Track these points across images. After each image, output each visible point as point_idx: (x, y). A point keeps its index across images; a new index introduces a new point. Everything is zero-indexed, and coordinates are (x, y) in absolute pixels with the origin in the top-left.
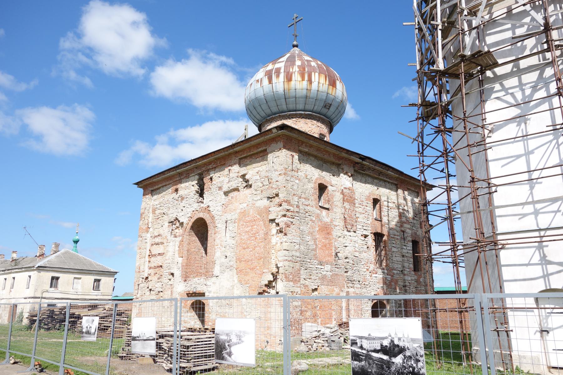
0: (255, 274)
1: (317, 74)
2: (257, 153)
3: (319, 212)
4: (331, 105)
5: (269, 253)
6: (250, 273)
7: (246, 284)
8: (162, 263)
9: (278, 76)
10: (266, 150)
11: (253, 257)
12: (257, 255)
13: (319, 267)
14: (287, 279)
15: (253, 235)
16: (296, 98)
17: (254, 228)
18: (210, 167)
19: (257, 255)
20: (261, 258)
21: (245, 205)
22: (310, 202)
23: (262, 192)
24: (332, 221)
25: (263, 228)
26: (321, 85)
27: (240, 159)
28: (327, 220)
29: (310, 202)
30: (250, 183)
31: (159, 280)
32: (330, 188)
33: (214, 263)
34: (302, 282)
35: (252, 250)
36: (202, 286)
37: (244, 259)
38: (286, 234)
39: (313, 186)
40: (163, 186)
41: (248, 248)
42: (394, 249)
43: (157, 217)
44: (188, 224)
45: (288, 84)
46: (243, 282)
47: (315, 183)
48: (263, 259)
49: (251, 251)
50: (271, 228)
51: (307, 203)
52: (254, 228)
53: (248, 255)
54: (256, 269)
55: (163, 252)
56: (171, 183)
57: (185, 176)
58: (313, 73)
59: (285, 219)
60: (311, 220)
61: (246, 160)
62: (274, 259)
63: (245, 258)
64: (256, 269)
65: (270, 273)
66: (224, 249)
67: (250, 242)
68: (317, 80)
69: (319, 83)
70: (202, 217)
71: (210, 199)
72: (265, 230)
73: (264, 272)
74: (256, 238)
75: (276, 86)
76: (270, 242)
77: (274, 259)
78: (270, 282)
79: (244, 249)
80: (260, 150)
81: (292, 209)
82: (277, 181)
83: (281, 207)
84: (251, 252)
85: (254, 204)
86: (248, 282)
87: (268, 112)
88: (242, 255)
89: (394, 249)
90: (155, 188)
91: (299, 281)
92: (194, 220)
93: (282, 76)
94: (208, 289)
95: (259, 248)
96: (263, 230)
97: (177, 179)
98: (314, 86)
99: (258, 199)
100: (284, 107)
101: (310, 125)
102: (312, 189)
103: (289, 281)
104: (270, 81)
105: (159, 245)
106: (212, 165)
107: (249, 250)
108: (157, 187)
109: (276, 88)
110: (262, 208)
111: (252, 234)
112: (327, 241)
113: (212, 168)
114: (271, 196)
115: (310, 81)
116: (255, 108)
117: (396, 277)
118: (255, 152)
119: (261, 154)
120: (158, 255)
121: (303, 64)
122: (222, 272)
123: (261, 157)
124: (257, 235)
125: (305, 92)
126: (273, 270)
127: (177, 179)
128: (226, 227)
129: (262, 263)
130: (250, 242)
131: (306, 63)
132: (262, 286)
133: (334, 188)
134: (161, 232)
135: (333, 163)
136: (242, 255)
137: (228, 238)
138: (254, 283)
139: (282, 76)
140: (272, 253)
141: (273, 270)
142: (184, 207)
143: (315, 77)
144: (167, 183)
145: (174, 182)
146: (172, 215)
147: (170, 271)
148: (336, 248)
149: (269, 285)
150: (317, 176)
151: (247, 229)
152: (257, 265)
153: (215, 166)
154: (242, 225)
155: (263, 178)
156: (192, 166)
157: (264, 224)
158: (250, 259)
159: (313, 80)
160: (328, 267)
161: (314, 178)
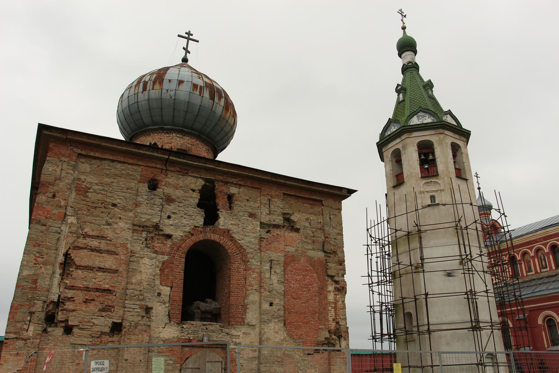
0: (309, 329)
2: (305, 198)
5: (325, 309)
6: (303, 327)
7: (299, 338)
8: (111, 286)
11: (306, 310)
12: (311, 309)
15: (305, 286)
16: (222, 129)
17: (307, 279)
18: (234, 180)
19: (311, 309)
20: (316, 313)
21: (293, 249)
23: (314, 242)
25: (317, 281)
30: (298, 226)
31: (104, 314)
35: (304, 301)
36: (220, 336)
37: (295, 311)
40: (113, 161)
41: (299, 298)
43: (94, 205)
44: (183, 240)
45: (225, 113)
46: (294, 337)
48: (318, 314)
49: (303, 303)
50: (327, 283)
52: (307, 279)
53: (300, 306)
54: (310, 324)
55: (114, 267)
56: (140, 165)
57: (178, 169)
61: (289, 198)
62: (331, 316)
63: (296, 309)
64: (310, 324)
65: (327, 330)
66: (268, 294)
67: (302, 293)
70: (218, 240)
71: (232, 222)
72: (319, 283)
73: (320, 328)
74: (309, 290)
75: (216, 106)
76: (326, 298)
77: (331, 316)
79: (294, 299)
80: (314, 197)
82: (336, 239)
83: (341, 267)
84: (304, 305)
85: (305, 252)
86: (302, 337)
88: (292, 305)
90: (92, 154)
92: (198, 240)
94: (234, 340)
95: (313, 302)
96: (318, 283)
97: (158, 166)
99: (309, 248)
105: (102, 253)
106: (237, 180)
107: (301, 301)
108: (97, 155)
109: (215, 109)
110: (316, 259)
111: (304, 285)
113: (235, 184)
114: (328, 252)
116: (174, 109)
118: (307, 196)
119: (311, 202)
120: (97, 270)
122: (262, 322)
123: (310, 204)
124: (311, 287)
126: (331, 327)
127: (158, 166)
128: (271, 268)
129: (317, 318)
130: (302, 293)
132: (320, 343)
134: (109, 234)
136: (292, 305)
137: (275, 281)
138: (309, 338)
140: (329, 310)
141: (331, 327)
142: (174, 213)
144: (130, 161)
145: (148, 166)
146: (150, 217)
147: (143, 303)
151: (298, 278)
152: (311, 319)
153: (242, 183)
154: (291, 271)
155: (314, 228)
156: (206, 165)
157: (319, 278)
158: (302, 311)
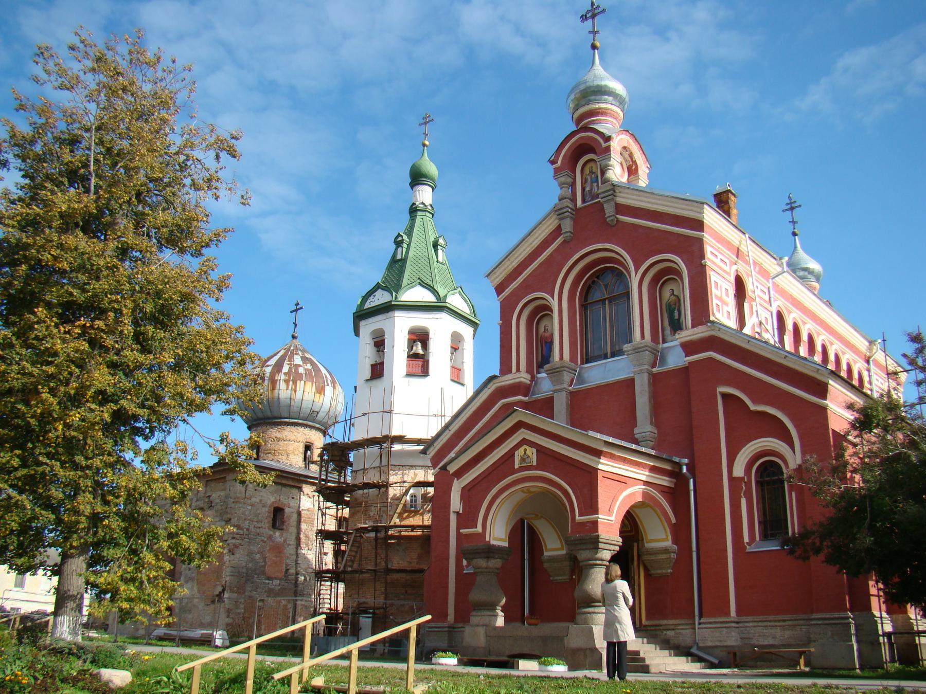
2: (220, 478)
3: (271, 533)
4: (318, 412)
10: (225, 477)
13: (267, 581)
14: (232, 591)
22: (262, 525)
24: (285, 541)
26: (306, 394)
27: (207, 481)
28: (281, 540)
29: (262, 525)
32: (287, 510)
33: (181, 573)
34: (246, 593)
38: (233, 554)
39: (267, 509)
47: (270, 507)
51: (259, 525)
58: (298, 382)
59: (234, 541)
60: (262, 541)
78: (220, 593)
81: (241, 532)
87: (255, 417)
91: (244, 593)
98: (299, 394)
100: (269, 414)
101: (295, 433)
102: (265, 513)
103: (233, 592)
112: (278, 559)
121: (290, 369)
133: (291, 510)
135: (294, 487)
148: (287, 565)
149: (220, 596)
150: (273, 499)
160: (277, 582)
161: (269, 502)
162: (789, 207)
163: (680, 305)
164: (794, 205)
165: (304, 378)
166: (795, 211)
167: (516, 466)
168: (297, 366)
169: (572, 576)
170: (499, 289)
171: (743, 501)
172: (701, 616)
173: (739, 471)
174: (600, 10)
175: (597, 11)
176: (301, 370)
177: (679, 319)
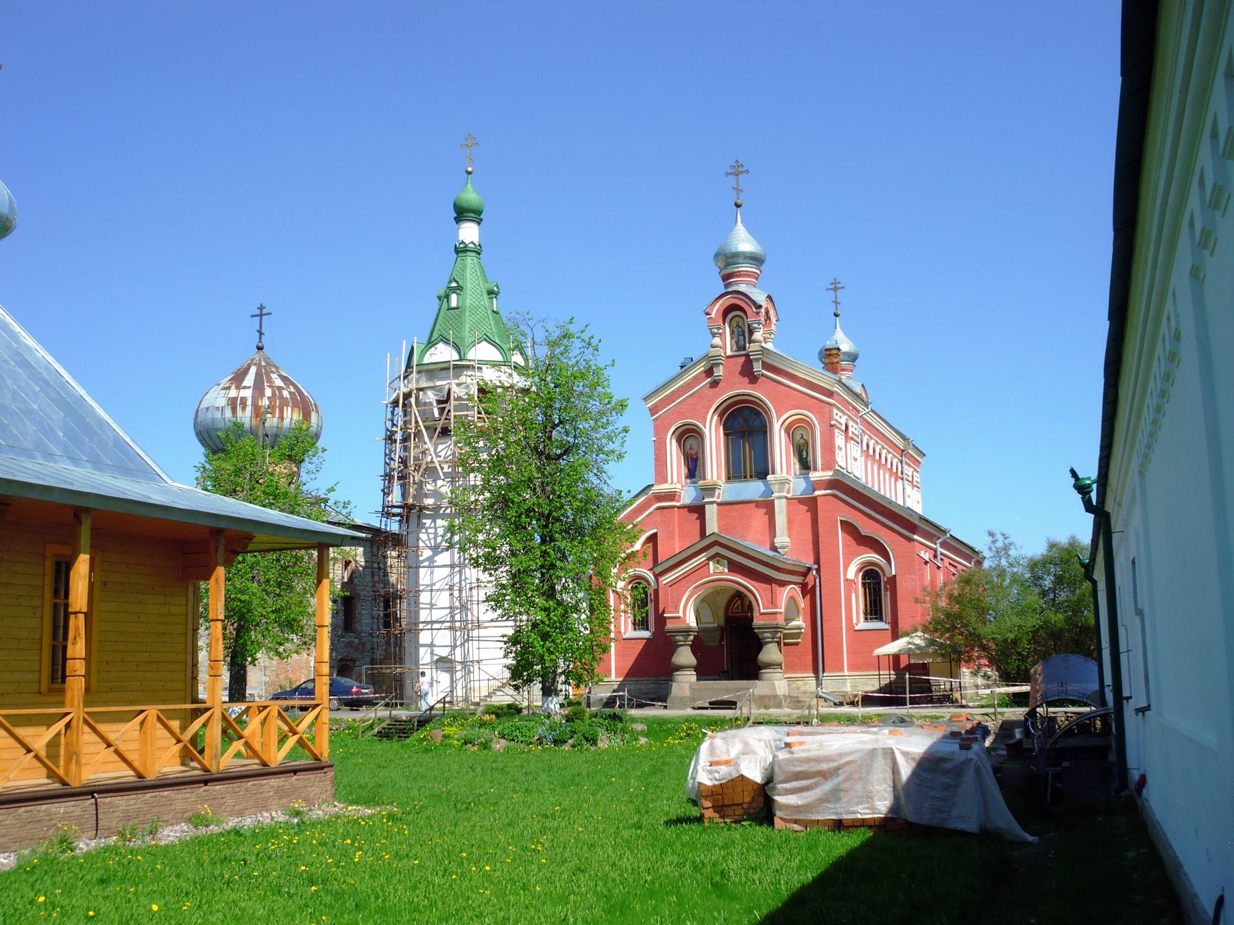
1: (290, 408)
9: (244, 408)
42: (364, 612)
58: (285, 408)
68: (290, 417)
69: (291, 419)
89: (364, 612)
93: (249, 409)
98: (286, 423)
104: (234, 410)
115: (282, 418)
117: (364, 640)
125: (275, 430)
131: (277, 392)
139: (249, 409)
143: (288, 412)
159: (285, 416)
162: (833, 286)
163: (807, 448)
164: (838, 286)
165: (291, 404)
166: (839, 292)
167: (711, 572)
168: (280, 388)
169: (720, 642)
170: (653, 411)
171: (853, 595)
172: (824, 672)
173: (851, 574)
174: (744, 169)
175: (740, 169)
176: (285, 394)
177: (807, 458)
